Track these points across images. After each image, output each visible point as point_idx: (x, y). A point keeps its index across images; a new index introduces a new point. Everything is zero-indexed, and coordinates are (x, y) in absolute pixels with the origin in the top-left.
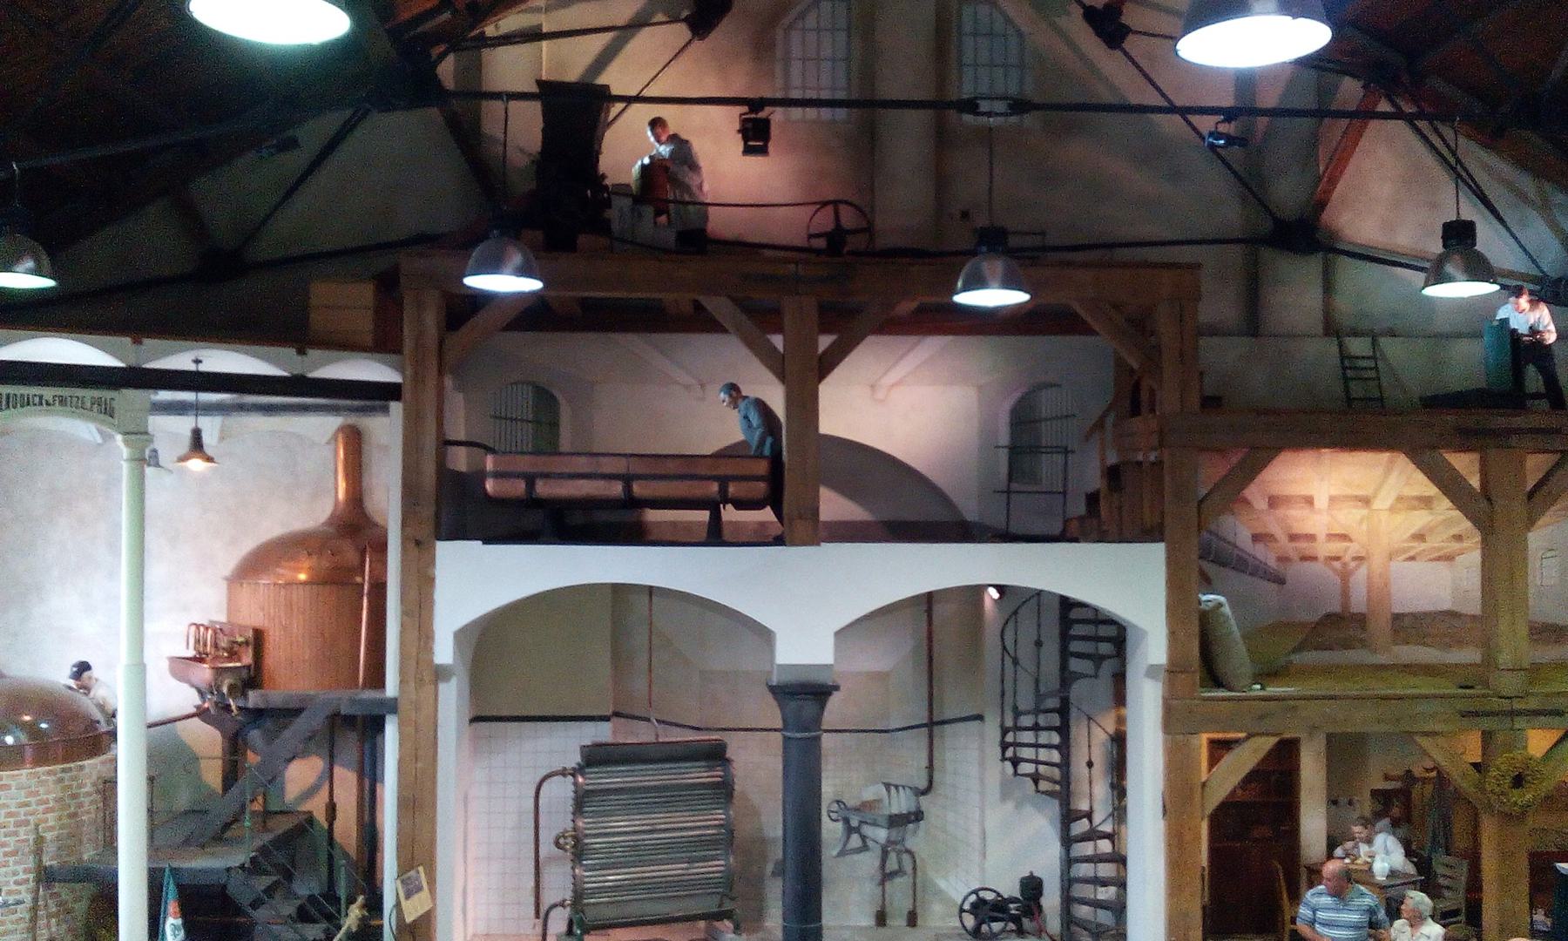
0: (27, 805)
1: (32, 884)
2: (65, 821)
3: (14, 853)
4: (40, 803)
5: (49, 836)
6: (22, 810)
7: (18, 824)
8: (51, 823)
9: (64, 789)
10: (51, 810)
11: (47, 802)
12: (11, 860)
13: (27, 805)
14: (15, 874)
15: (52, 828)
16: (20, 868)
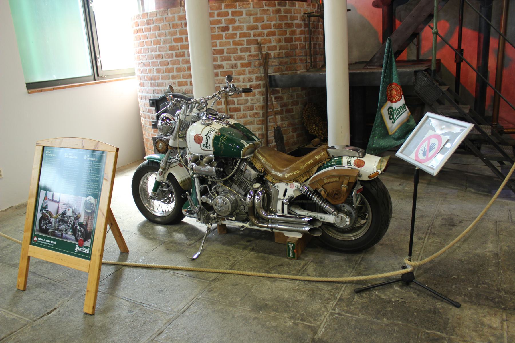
0: (255, 28)
1: (262, 89)
2: (283, 43)
3: (249, 65)
4: (264, 27)
5: (272, 53)
6: (252, 32)
7: (249, 42)
8: (273, 44)
9: (281, 18)
10: (273, 34)
11: (269, 27)
12: (247, 69)
13: (255, 28)
14: (250, 80)
15: (275, 48)
16: (254, 76)
